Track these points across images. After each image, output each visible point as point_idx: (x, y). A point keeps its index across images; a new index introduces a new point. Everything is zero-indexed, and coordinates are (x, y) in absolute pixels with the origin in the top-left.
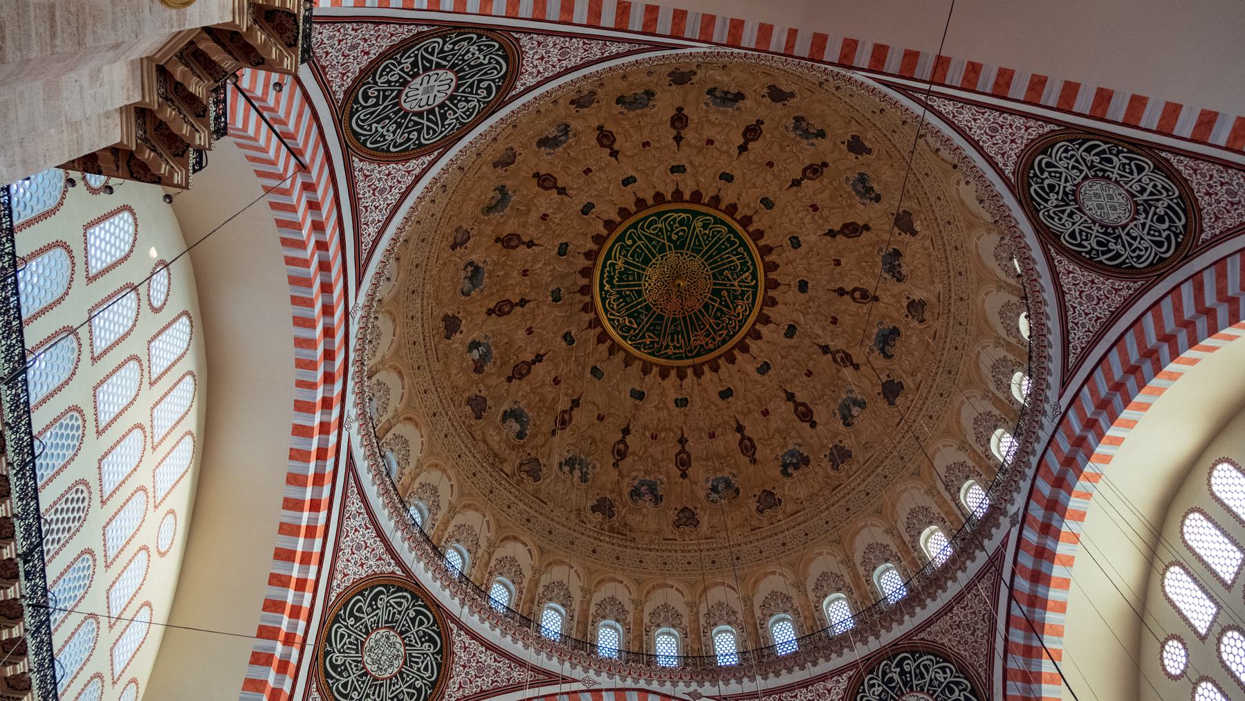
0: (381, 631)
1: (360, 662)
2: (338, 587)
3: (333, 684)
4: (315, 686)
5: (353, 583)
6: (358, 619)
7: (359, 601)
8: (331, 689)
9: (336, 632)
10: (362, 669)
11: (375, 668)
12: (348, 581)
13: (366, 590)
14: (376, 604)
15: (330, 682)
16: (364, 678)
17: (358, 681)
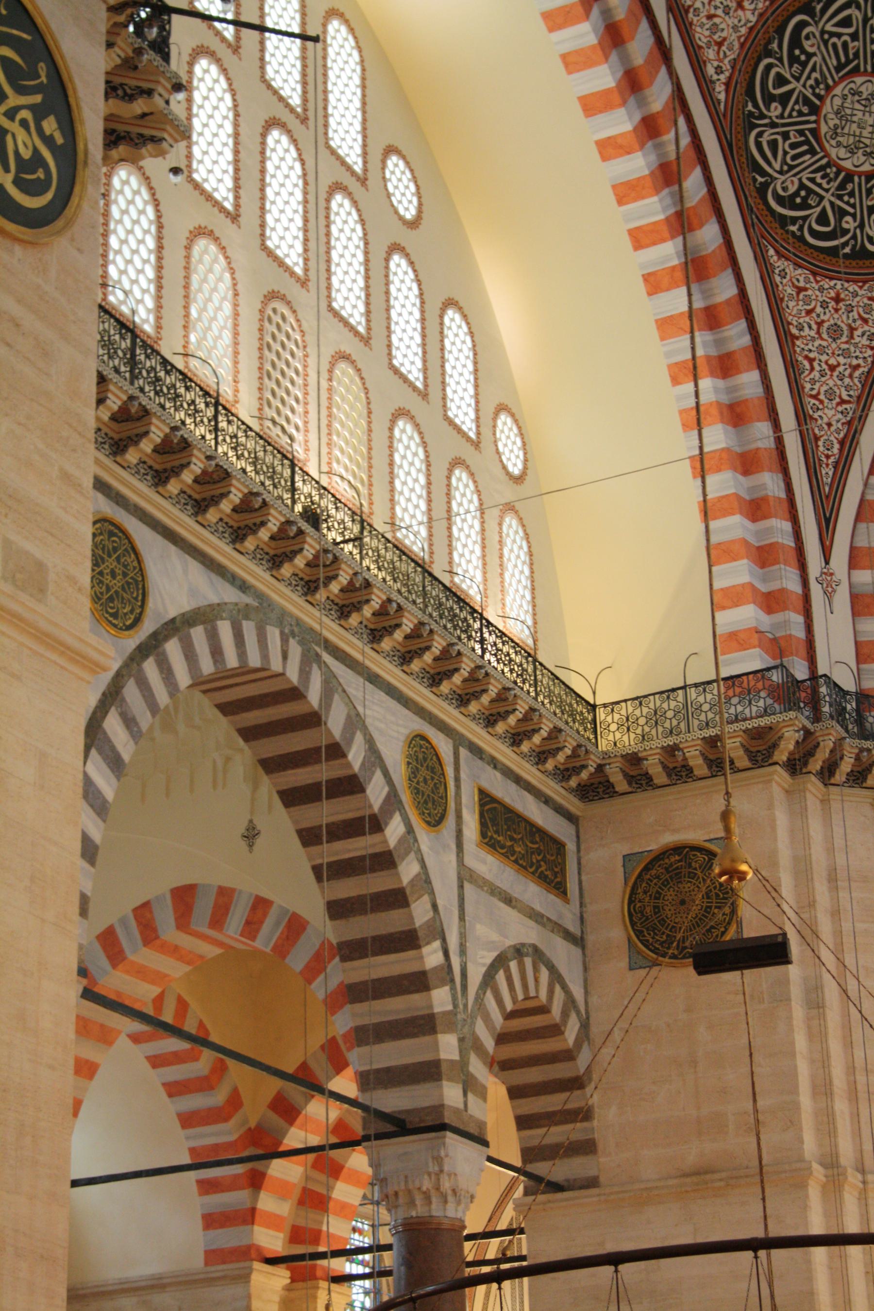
0: (838, 91)
1: (828, 165)
2: (719, 70)
3: (801, 229)
4: (771, 252)
5: (742, 45)
6: (784, 100)
7: (769, 67)
8: (802, 239)
9: (759, 145)
10: (837, 174)
11: (860, 157)
12: (730, 49)
13: (770, 42)
14: (803, 51)
15: (794, 228)
16: (849, 187)
17: (840, 197)
